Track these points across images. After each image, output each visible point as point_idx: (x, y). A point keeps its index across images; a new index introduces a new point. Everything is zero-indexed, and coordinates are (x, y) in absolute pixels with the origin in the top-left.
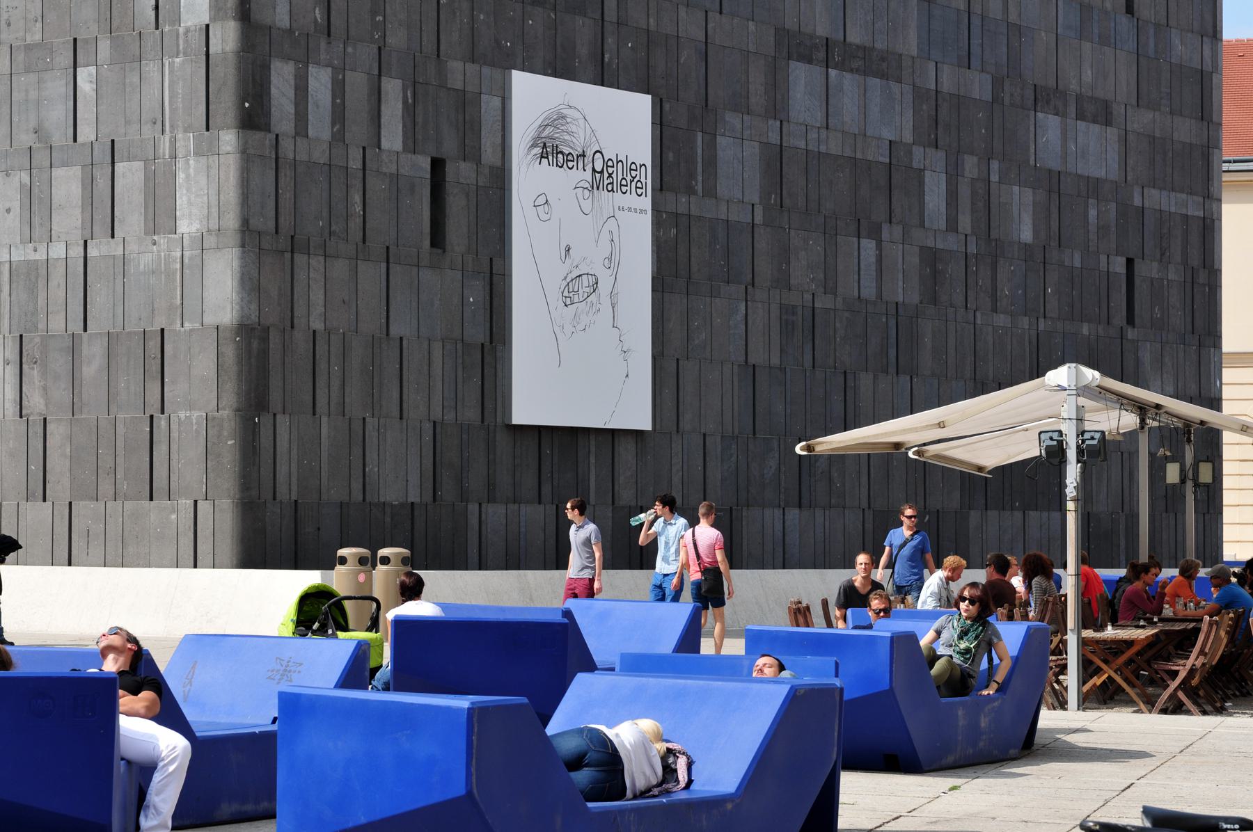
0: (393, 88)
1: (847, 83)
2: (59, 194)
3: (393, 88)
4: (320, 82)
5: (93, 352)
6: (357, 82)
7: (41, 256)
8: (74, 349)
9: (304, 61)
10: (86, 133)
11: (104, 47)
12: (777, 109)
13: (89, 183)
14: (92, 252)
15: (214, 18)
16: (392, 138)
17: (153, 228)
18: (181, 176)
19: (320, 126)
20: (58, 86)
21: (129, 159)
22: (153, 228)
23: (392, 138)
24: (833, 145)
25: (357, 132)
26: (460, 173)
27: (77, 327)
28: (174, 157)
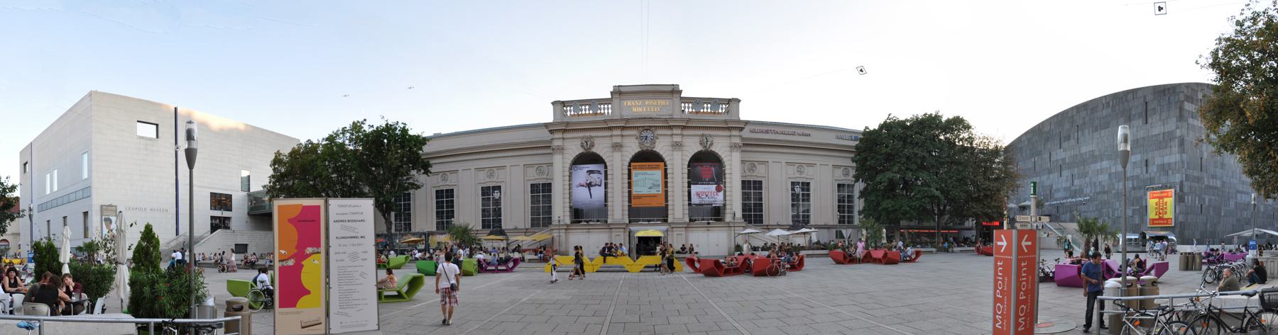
0: (1197, 198)
1: (1243, 195)
3: (1197, 198)
4: (1190, 198)
6: (1193, 197)
9: (1188, 196)
12: (1236, 198)
16: (1197, 203)
19: (1190, 201)
23: (1197, 203)
24: (1242, 202)
25: (1193, 202)
26: (1203, 206)
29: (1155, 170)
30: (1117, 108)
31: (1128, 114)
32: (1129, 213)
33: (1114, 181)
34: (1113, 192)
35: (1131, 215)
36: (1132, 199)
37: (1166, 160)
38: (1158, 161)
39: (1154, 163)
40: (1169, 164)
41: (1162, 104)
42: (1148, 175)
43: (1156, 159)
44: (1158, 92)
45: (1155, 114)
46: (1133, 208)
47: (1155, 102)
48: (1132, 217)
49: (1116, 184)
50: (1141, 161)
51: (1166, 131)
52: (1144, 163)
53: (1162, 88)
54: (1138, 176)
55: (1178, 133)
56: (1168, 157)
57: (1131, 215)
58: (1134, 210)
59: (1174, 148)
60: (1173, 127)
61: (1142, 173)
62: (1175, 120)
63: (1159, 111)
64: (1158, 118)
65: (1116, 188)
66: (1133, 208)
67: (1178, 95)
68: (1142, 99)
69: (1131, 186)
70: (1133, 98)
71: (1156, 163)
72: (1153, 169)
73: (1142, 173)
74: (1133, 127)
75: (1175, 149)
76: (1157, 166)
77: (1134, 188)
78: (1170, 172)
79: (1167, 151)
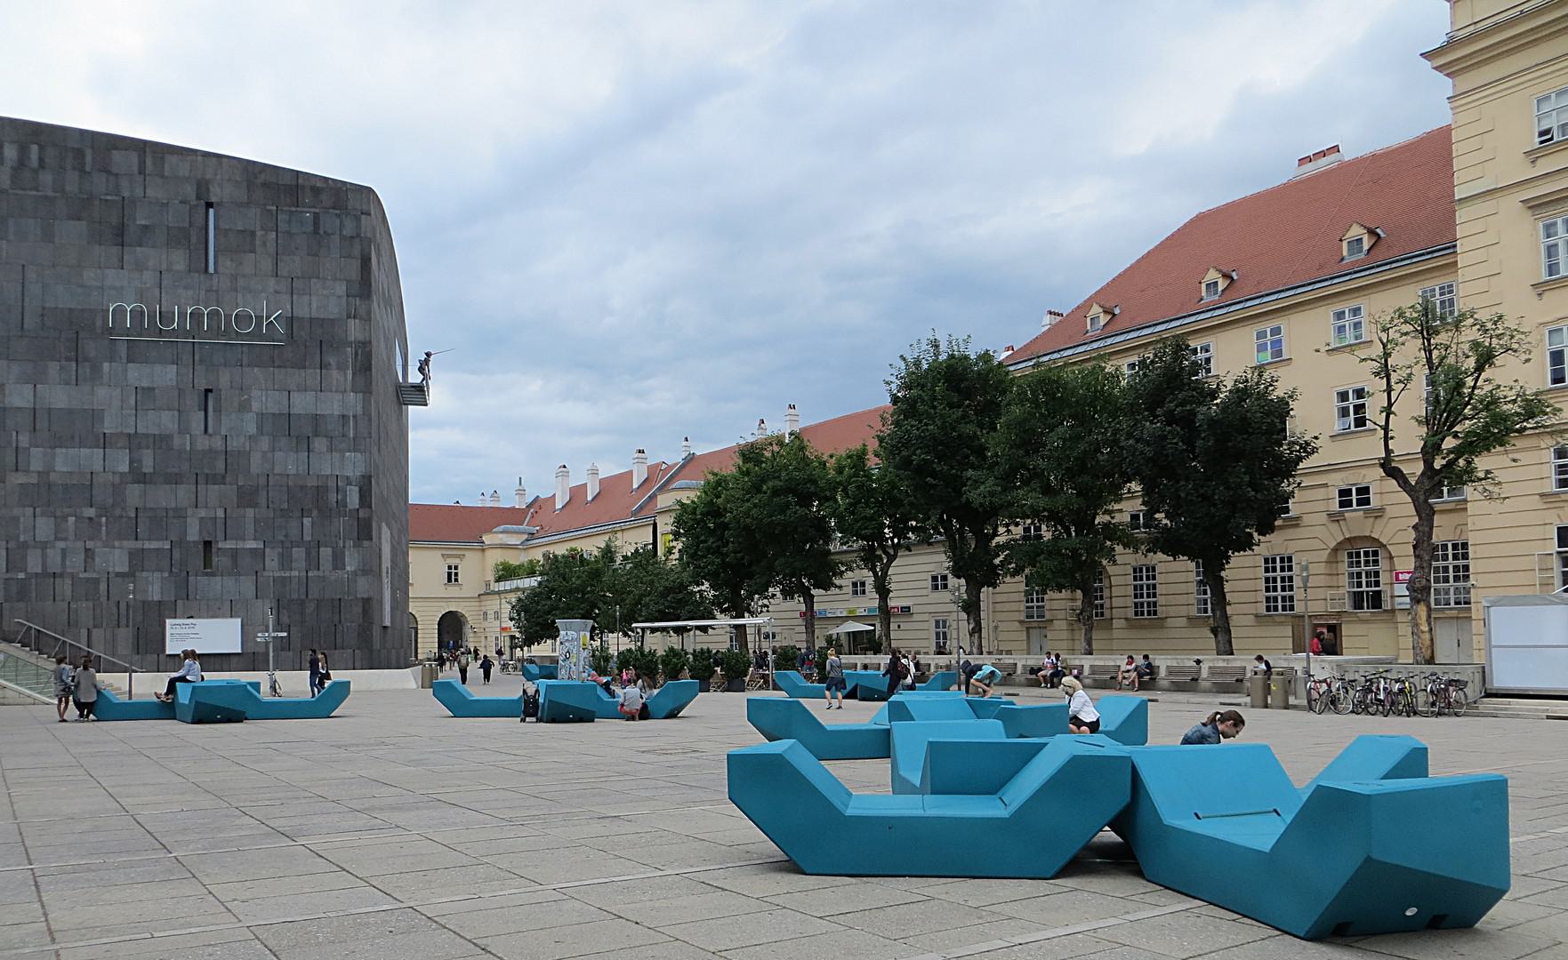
2: (295, 556)
5: (310, 608)
7: (287, 574)
8: (302, 603)
10: (307, 538)
11: (315, 513)
13: (308, 554)
14: (310, 574)
15: (361, 507)
17: (335, 567)
18: (347, 553)
20: (294, 524)
21: (326, 547)
22: (335, 567)
27: (303, 597)
28: (344, 547)
29: (252, 429)
30: (47, 178)
31: (114, 220)
32: (115, 559)
33: (24, 440)
34: (20, 479)
35: (126, 569)
36: (133, 515)
37: (303, 403)
38: (265, 400)
39: (244, 407)
40: (316, 419)
41: (283, 226)
42: (218, 444)
43: (255, 393)
44: (264, 184)
45: (253, 251)
46: (131, 544)
47: (254, 212)
48: (130, 575)
49: (37, 453)
50: (181, 392)
51: (302, 312)
52: (192, 400)
53: (287, 180)
54: (161, 441)
55: (354, 330)
56: (310, 396)
57: (123, 568)
58: (138, 560)
59: (335, 373)
60: (334, 309)
61: (184, 430)
62: (341, 289)
63: (272, 250)
64: (267, 265)
65: (36, 464)
66: (139, 545)
67: (358, 219)
68: (190, 191)
69: (125, 468)
70: (142, 171)
71: (256, 406)
72: (238, 427)
73: (184, 430)
74: (140, 267)
75: (340, 377)
76: (261, 416)
77: (138, 476)
78: (319, 444)
79: (311, 375)
